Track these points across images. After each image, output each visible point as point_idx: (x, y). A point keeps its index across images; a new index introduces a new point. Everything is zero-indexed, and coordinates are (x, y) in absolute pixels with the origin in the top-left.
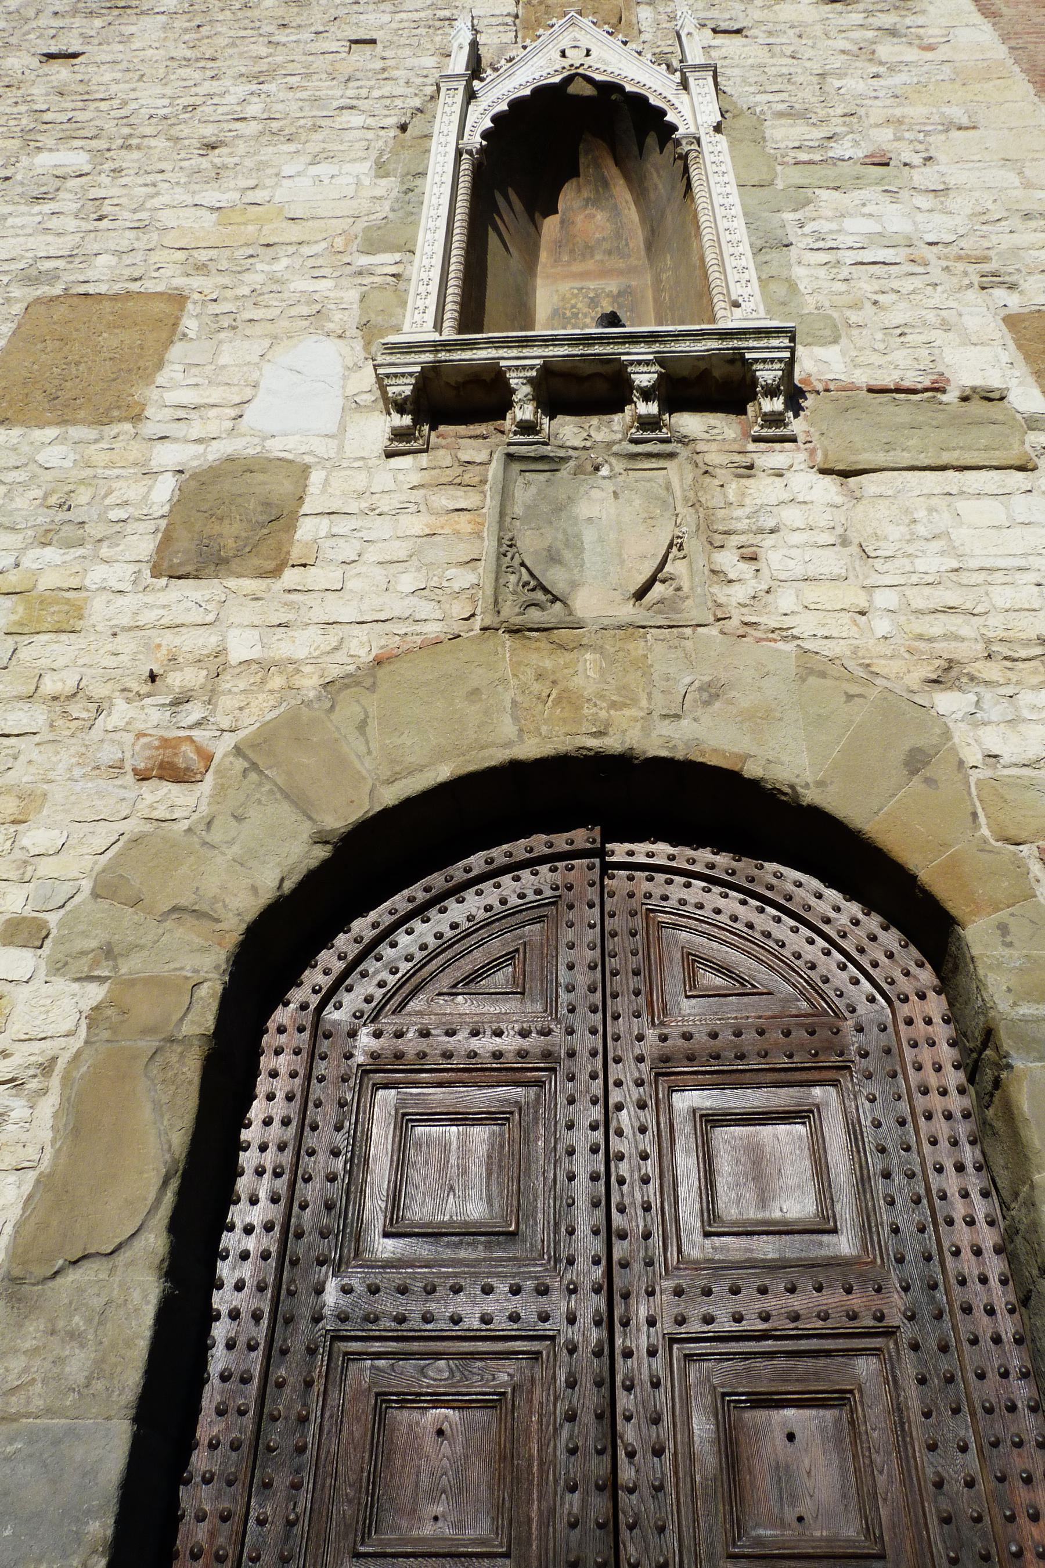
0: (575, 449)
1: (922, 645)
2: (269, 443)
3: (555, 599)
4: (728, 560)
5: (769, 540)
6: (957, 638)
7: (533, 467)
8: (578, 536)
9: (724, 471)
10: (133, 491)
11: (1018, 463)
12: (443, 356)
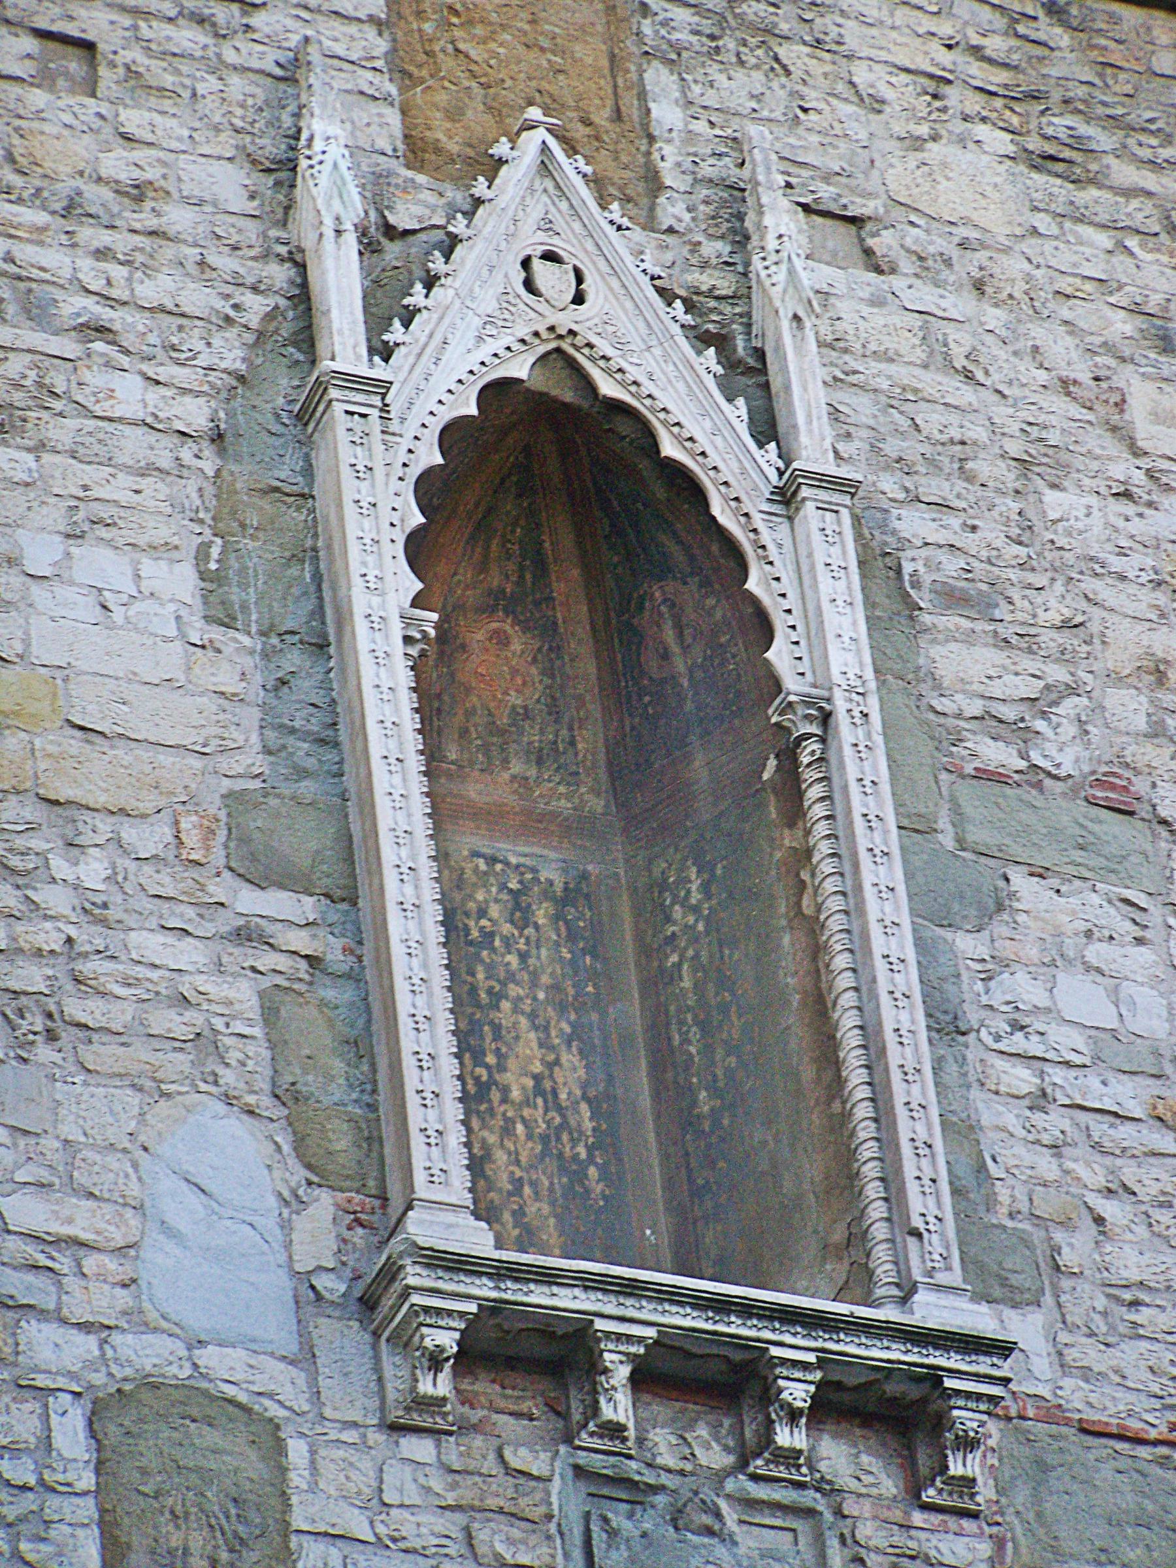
2: (208, 1357)
7: (605, 1491)
9: (880, 1558)
12: (512, 1292)
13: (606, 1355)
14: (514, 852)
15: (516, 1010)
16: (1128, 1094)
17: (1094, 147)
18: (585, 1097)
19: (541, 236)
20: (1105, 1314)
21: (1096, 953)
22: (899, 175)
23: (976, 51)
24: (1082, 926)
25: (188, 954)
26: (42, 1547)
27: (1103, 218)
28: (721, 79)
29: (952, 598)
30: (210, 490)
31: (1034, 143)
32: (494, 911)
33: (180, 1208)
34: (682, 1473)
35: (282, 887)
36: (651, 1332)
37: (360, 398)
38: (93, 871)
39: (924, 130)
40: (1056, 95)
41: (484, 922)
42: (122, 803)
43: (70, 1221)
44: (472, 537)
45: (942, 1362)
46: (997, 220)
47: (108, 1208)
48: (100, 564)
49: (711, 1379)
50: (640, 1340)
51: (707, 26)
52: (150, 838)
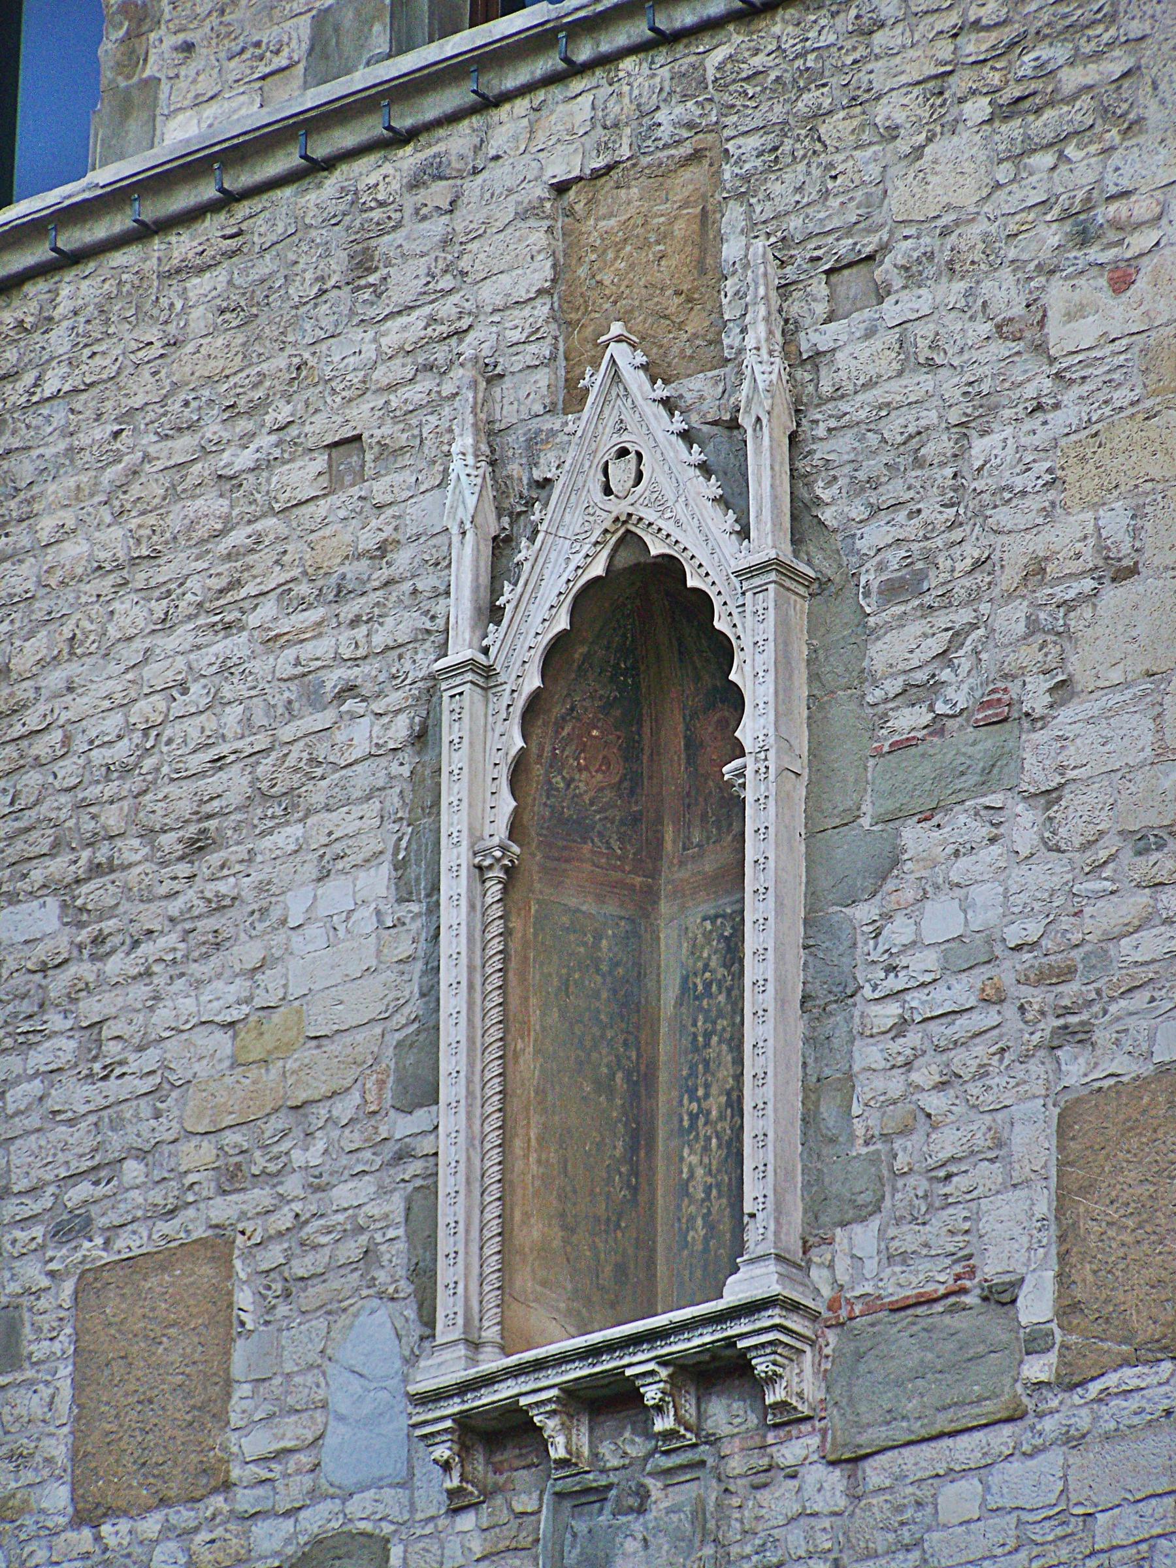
7: (583, 1500)
11: (1004, 1415)
13: (536, 1419)
15: (720, 1042)
16: (960, 991)
19: (616, 439)
21: (959, 870)
22: (901, 198)
24: (950, 849)
29: (893, 591)
30: (407, 787)
34: (624, 1467)
35: (421, 1106)
36: (554, 1392)
37: (458, 680)
38: (313, 1155)
41: (707, 975)
42: (334, 1087)
44: (681, 661)
45: (730, 1333)
46: (967, 197)
47: (305, 1415)
48: (336, 894)
49: (607, 1400)
50: (549, 1400)
51: (770, 140)
52: (344, 1109)
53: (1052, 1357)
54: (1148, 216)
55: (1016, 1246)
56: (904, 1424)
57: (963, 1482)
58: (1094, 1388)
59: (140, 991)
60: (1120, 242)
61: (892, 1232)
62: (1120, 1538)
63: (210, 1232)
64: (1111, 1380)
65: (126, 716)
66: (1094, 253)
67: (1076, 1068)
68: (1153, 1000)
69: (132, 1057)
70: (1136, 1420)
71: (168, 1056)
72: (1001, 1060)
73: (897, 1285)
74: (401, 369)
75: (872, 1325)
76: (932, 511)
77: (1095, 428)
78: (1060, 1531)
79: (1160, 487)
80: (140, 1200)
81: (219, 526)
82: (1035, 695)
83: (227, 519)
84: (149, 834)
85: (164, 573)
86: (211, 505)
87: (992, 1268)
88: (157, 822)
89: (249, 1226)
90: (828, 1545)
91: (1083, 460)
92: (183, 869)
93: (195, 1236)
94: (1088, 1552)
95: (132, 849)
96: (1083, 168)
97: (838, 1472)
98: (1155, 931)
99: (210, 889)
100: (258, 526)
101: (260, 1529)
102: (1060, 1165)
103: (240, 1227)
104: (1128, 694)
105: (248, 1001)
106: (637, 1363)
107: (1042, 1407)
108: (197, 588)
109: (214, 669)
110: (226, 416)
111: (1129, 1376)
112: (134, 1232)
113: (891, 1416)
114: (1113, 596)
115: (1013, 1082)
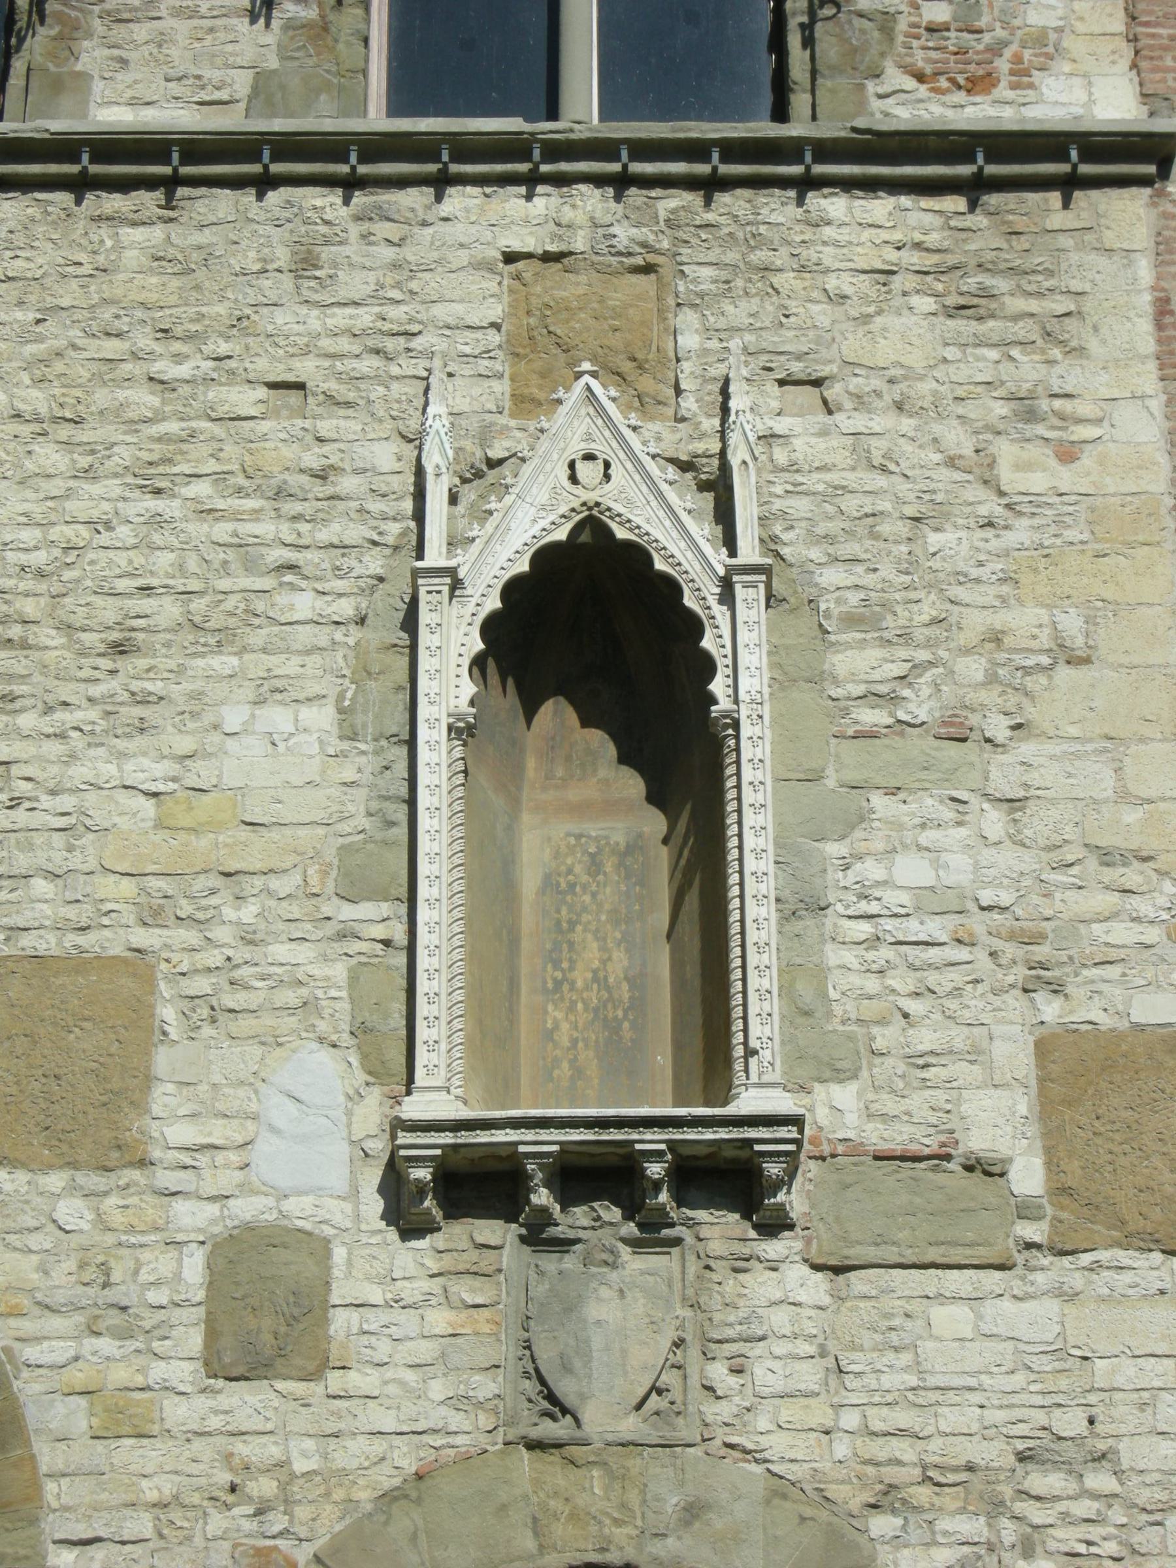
0: (585, 1228)
1: (870, 1470)
2: (290, 1205)
3: (565, 1411)
4: (718, 1372)
5: (759, 1349)
6: (899, 1463)
8: (587, 1341)
10: (161, 1263)
11: (996, 1261)
14: (593, 829)
15: (585, 930)
16: (936, 928)
17: (996, 292)
18: (626, 978)
19: (583, 445)
20: (903, 1077)
21: (928, 837)
22: (852, 345)
23: (918, 246)
24: (917, 821)
25: (303, 953)
26: (167, 1342)
27: (995, 338)
28: (729, 309)
29: (851, 621)
30: (351, 654)
31: (953, 300)
32: (578, 869)
33: (280, 1111)
34: (593, 1228)
35: (369, 899)
36: (555, 1148)
37: (436, 581)
38: (248, 913)
39: (871, 309)
40: (973, 262)
41: (571, 877)
42: (272, 866)
43: (210, 1134)
46: (916, 360)
47: (236, 1122)
51: (724, 275)
53: (1045, 1225)
54: (1092, 416)
55: (1000, 1132)
56: (895, 1249)
57: (952, 1307)
58: (1086, 1259)
59: (54, 748)
60: (1060, 428)
61: (871, 1096)
62: (1120, 1381)
63: (128, 954)
64: (1103, 1255)
65: (45, 534)
66: (1040, 430)
67: (1051, 1009)
68: (1124, 975)
69: (44, 798)
70: (1130, 1292)
71: (87, 804)
72: (975, 989)
73: (876, 1136)
74: (345, 344)
75: (855, 1164)
76: (887, 571)
77: (1046, 551)
78: (1058, 1365)
79: (1111, 607)
80: (49, 912)
81: (150, 415)
82: (998, 727)
83: (156, 411)
84: (68, 628)
85: (84, 435)
86: (145, 399)
87: (977, 1142)
88: (78, 620)
89: (175, 957)
90: (814, 1331)
91: (1036, 570)
92: (105, 663)
93: (111, 953)
94: (1088, 1387)
95: (48, 636)
96: (1027, 370)
97: (820, 1275)
98: (1123, 925)
99: (136, 686)
100: (194, 424)
101: (180, 1206)
102: (1042, 1081)
103: (165, 955)
104: (1089, 747)
105: (174, 779)
106: (651, 1140)
107: (1033, 1262)
108: (125, 455)
109: (142, 519)
110: (159, 335)
111: (1123, 1257)
112: (41, 937)
113: (880, 1241)
114: (1064, 673)
115: (989, 1007)
